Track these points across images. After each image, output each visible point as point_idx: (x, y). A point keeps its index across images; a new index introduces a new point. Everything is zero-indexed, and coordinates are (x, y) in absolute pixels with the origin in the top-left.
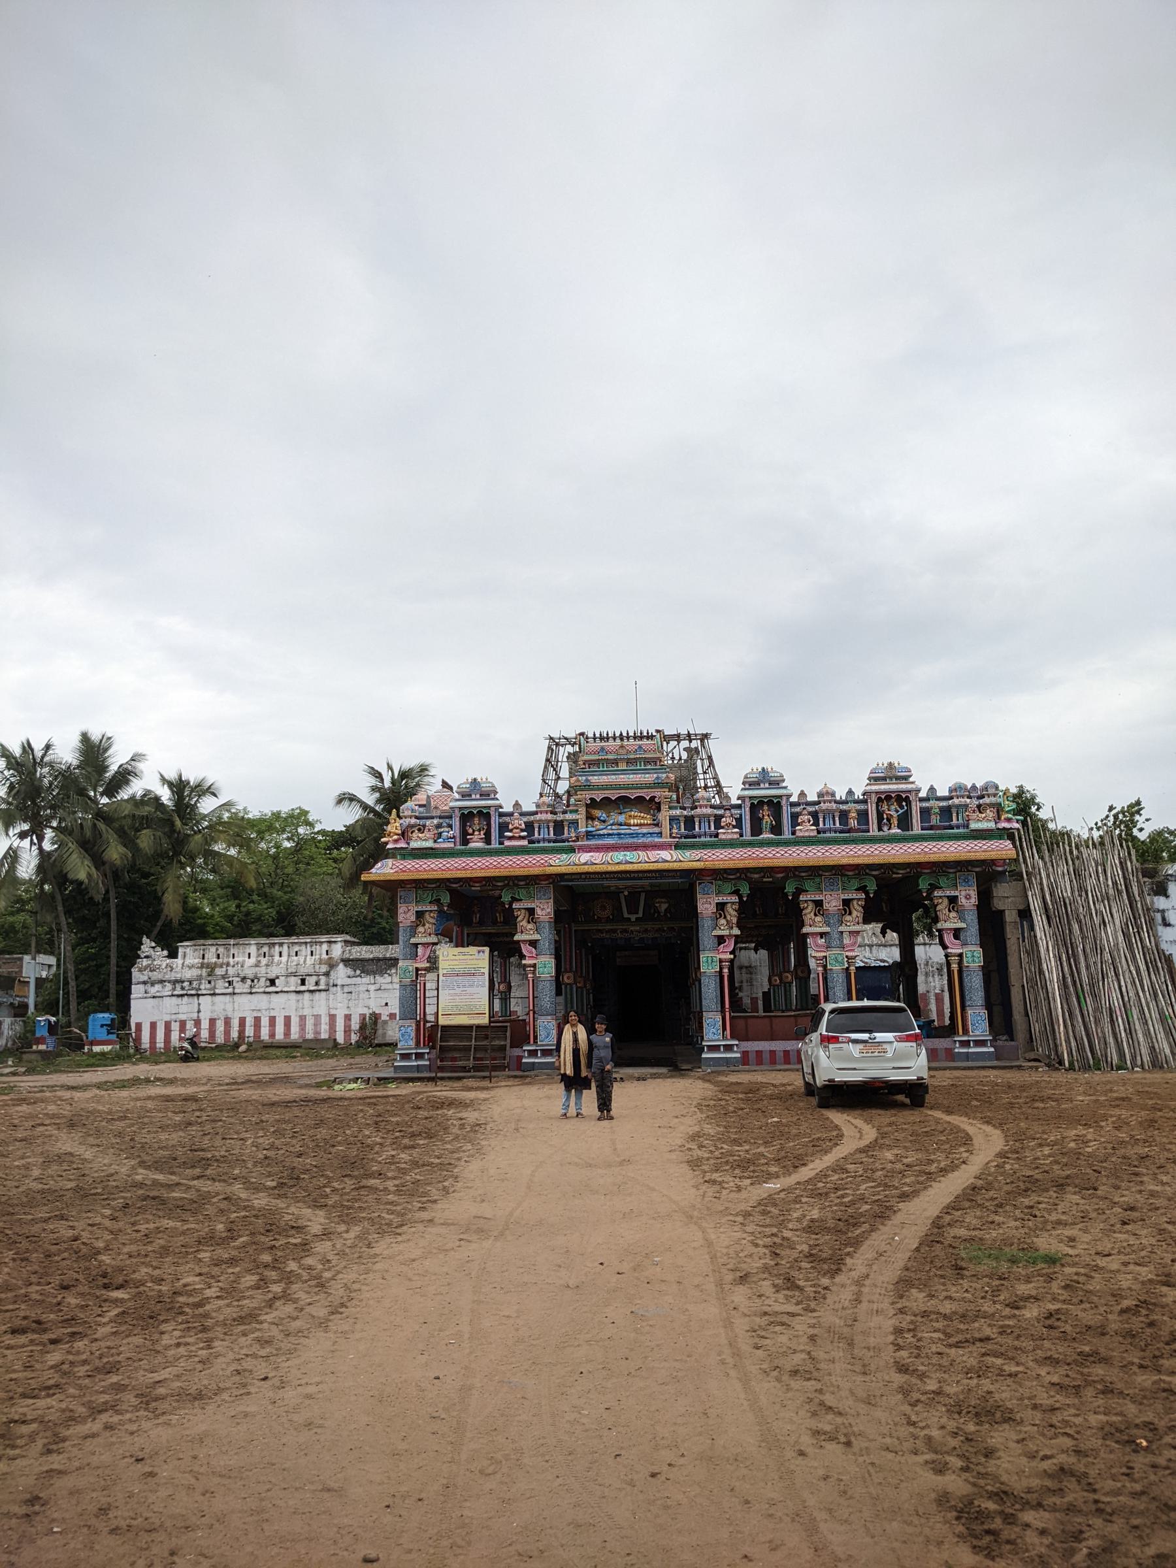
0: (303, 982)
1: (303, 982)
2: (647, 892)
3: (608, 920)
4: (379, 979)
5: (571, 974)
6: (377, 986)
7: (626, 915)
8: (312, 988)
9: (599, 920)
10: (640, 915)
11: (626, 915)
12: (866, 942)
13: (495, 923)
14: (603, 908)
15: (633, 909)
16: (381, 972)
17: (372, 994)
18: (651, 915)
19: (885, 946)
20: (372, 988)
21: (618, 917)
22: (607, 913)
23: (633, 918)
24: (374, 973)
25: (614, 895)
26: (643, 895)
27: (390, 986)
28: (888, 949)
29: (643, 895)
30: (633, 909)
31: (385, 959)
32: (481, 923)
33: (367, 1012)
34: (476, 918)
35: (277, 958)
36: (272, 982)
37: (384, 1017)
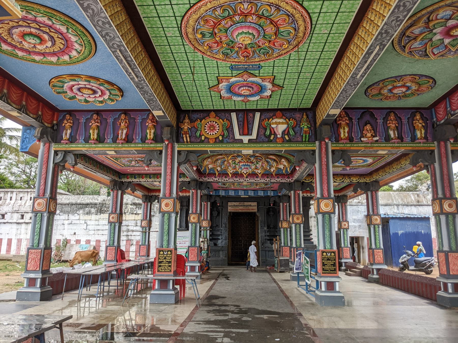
0: (22, 217)
1: (22, 217)
2: (262, 111)
3: (216, 141)
4: (71, 217)
5: (170, 202)
6: (69, 222)
7: (237, 136)
8: (27, 221)
9: (207, 141)
10: (254, 136)
11: (237, 136)
12: (395, 202)
13: (87, 140)
14: (212, 128)
15: (246, 129)
16: (73, 212)
17: (66, 226)
18: (266, 136)
19: (407, 205)
20: (66, 222)
21: (227, 136)
22: (216, 132)
23: (246, 139)
24: (68, 213)
25: (223, 113)
26: (258, 115)
27: (78, 222)
28: (409, 208)
29: (258, 115)
30: (246, 129)
31: (76, 204)
32: (72, 140)
33: (62, 238)
34: (66, 134)
35: (8, 201)
36: (3, 216)
37: (73, 242)
